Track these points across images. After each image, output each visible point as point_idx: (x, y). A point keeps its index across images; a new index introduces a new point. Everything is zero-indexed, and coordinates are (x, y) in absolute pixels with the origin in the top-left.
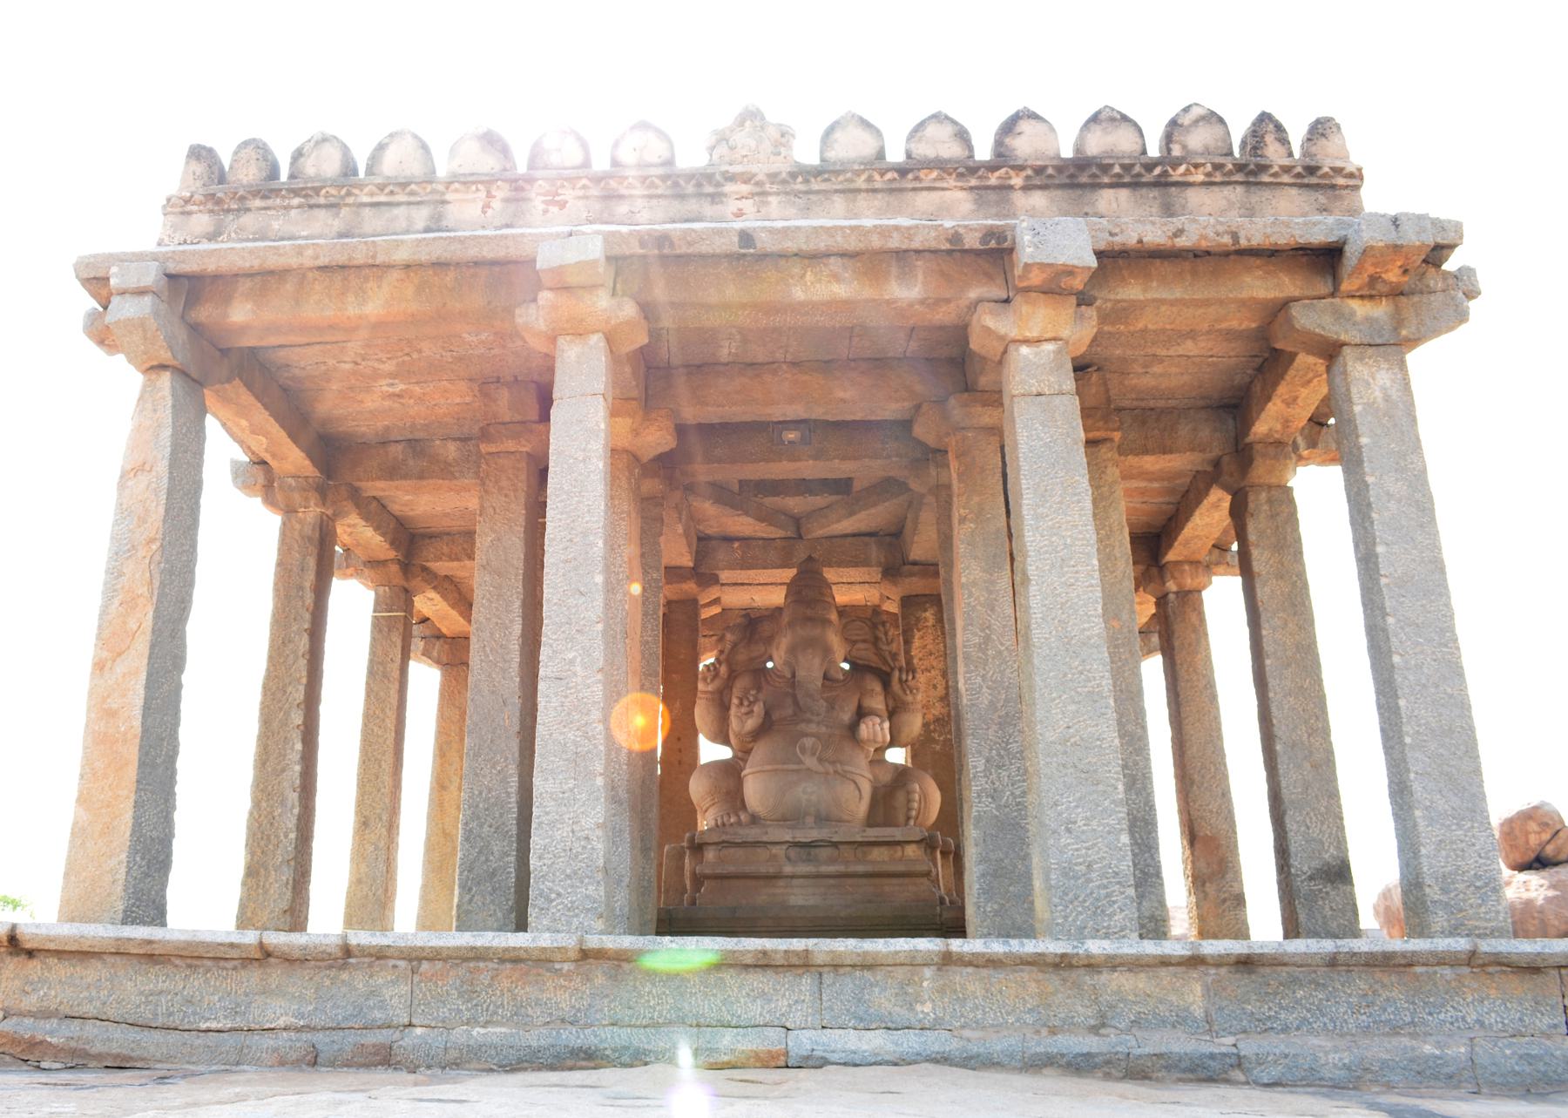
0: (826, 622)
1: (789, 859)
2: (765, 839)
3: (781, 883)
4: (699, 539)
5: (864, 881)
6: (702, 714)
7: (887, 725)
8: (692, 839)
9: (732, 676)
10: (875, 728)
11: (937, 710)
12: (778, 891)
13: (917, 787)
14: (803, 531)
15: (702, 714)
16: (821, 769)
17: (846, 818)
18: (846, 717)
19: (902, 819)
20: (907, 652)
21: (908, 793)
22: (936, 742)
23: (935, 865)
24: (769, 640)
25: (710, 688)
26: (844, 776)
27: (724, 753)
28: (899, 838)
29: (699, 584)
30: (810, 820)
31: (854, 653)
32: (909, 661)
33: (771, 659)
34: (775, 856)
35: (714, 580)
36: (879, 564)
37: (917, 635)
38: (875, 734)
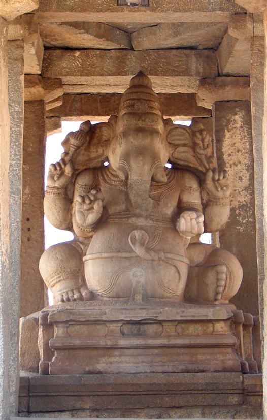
0: (154, 132)
1: (123, 333)
2: (104, 318)
3: (117, 353)
4: (46, 48)
5: (182, 350)
6: (50, 207)
7: (202, 219)
8: (45, 317)
9: (76, 174)
10: (190, 222)
11: (243, 198)
12: (113, 359)
13: (224, 268)
14: (134, 43)
15: (50, 207)
16: (148, 257)
17: (168, 295)
18: (169, 210)
19: (211, 294)
20: (219, 149)
21: (218, 273)
22: (240, 224)
23: (238, 337)
24: (107, 143)
25: (57, 185)
26: (167, 261)
27: (67, 236)
28: (211, 317)
29: (45, 88)
30: (139, 297)
31: (176, 155)
32: (220, 158)
33: (107, 160)
34: (112, 331)
35: (59, 84)
36: (198, 73)
37: (228, 134)
38: (192, 227)
